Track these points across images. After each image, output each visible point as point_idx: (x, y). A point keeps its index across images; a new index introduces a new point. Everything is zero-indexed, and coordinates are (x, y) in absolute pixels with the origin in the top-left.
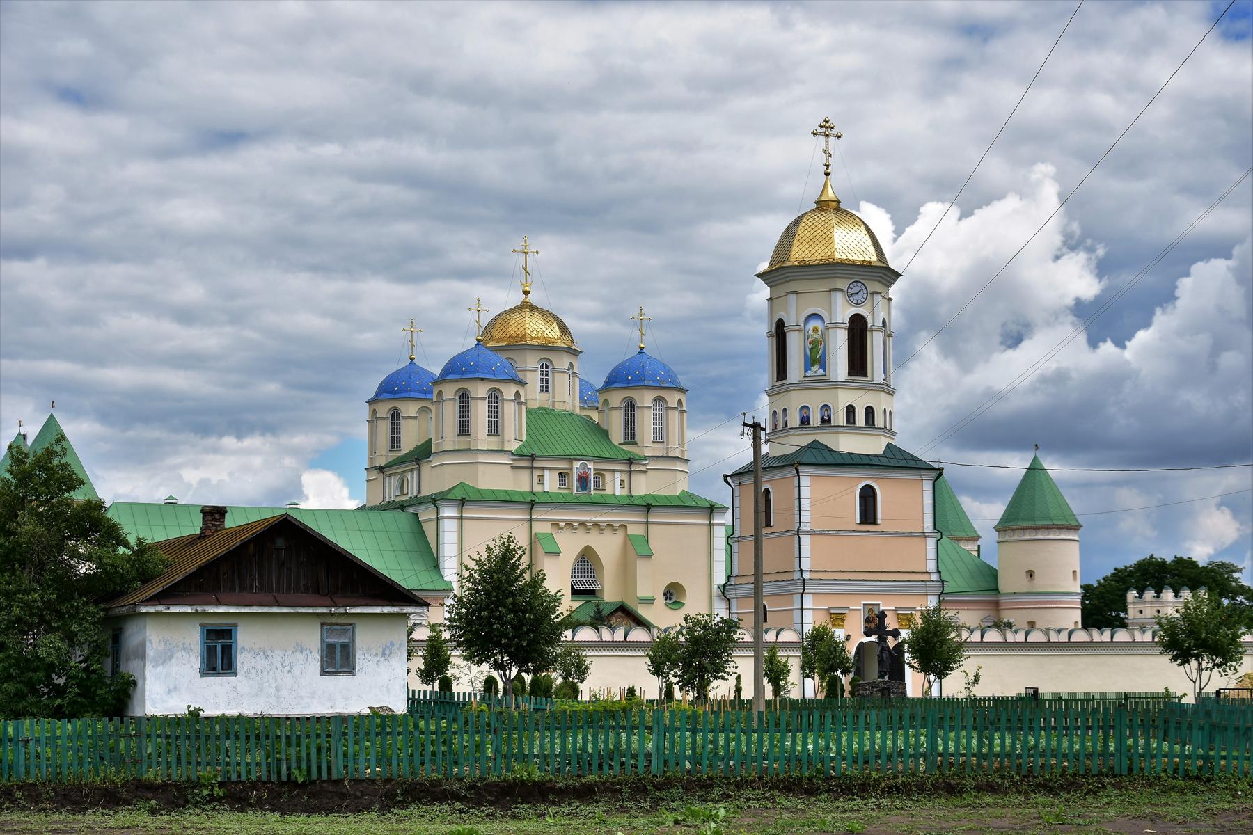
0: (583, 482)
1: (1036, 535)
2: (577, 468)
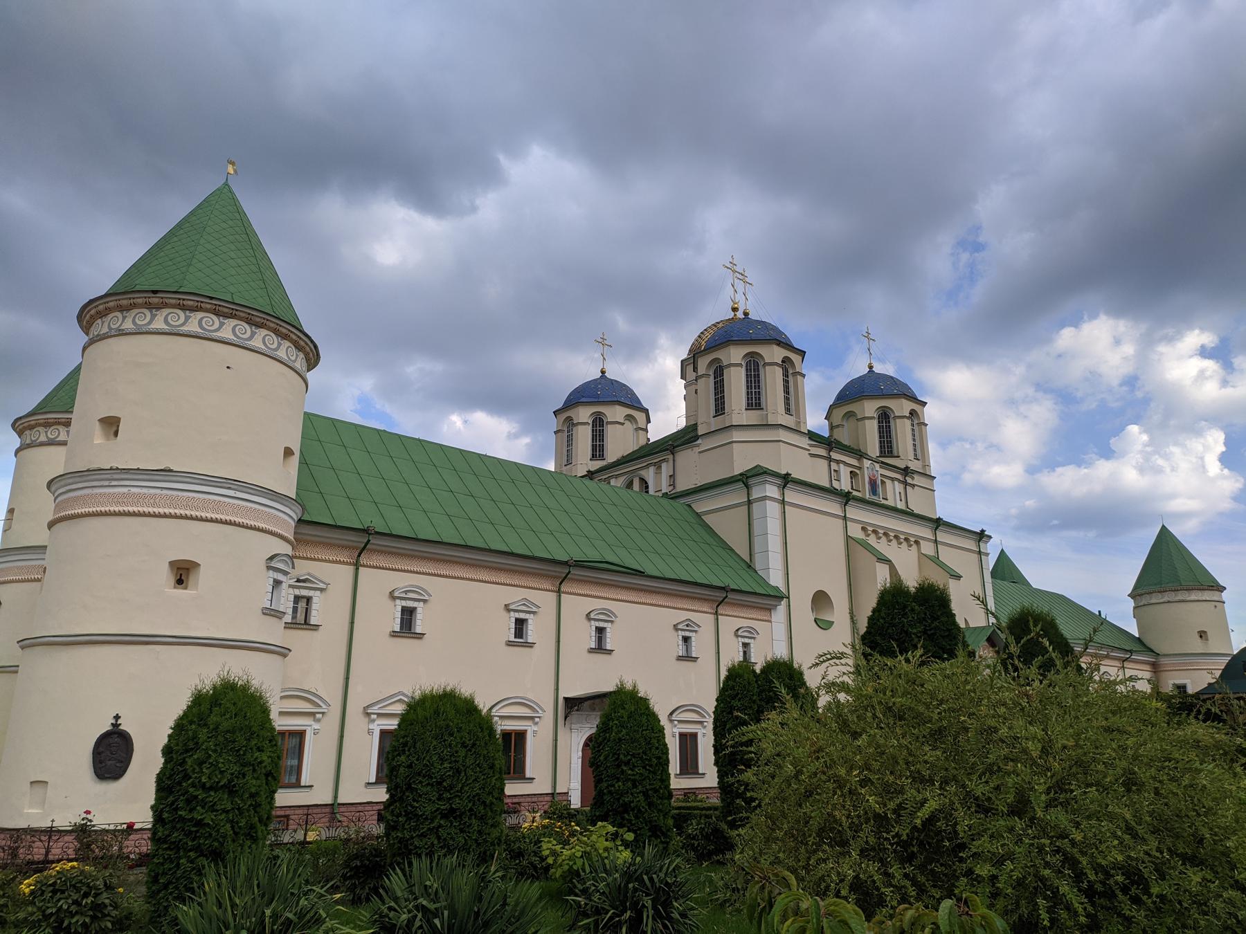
0: (873, 484)
1: (1189, 596)
2: (868, 468)
